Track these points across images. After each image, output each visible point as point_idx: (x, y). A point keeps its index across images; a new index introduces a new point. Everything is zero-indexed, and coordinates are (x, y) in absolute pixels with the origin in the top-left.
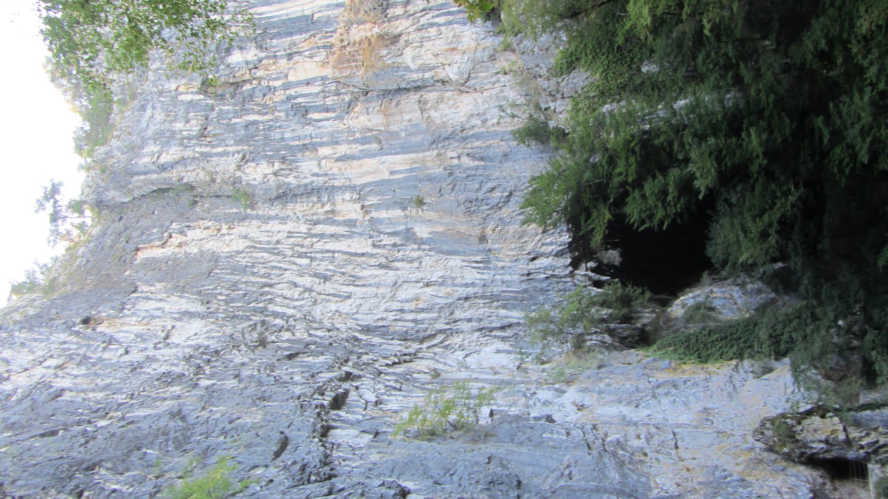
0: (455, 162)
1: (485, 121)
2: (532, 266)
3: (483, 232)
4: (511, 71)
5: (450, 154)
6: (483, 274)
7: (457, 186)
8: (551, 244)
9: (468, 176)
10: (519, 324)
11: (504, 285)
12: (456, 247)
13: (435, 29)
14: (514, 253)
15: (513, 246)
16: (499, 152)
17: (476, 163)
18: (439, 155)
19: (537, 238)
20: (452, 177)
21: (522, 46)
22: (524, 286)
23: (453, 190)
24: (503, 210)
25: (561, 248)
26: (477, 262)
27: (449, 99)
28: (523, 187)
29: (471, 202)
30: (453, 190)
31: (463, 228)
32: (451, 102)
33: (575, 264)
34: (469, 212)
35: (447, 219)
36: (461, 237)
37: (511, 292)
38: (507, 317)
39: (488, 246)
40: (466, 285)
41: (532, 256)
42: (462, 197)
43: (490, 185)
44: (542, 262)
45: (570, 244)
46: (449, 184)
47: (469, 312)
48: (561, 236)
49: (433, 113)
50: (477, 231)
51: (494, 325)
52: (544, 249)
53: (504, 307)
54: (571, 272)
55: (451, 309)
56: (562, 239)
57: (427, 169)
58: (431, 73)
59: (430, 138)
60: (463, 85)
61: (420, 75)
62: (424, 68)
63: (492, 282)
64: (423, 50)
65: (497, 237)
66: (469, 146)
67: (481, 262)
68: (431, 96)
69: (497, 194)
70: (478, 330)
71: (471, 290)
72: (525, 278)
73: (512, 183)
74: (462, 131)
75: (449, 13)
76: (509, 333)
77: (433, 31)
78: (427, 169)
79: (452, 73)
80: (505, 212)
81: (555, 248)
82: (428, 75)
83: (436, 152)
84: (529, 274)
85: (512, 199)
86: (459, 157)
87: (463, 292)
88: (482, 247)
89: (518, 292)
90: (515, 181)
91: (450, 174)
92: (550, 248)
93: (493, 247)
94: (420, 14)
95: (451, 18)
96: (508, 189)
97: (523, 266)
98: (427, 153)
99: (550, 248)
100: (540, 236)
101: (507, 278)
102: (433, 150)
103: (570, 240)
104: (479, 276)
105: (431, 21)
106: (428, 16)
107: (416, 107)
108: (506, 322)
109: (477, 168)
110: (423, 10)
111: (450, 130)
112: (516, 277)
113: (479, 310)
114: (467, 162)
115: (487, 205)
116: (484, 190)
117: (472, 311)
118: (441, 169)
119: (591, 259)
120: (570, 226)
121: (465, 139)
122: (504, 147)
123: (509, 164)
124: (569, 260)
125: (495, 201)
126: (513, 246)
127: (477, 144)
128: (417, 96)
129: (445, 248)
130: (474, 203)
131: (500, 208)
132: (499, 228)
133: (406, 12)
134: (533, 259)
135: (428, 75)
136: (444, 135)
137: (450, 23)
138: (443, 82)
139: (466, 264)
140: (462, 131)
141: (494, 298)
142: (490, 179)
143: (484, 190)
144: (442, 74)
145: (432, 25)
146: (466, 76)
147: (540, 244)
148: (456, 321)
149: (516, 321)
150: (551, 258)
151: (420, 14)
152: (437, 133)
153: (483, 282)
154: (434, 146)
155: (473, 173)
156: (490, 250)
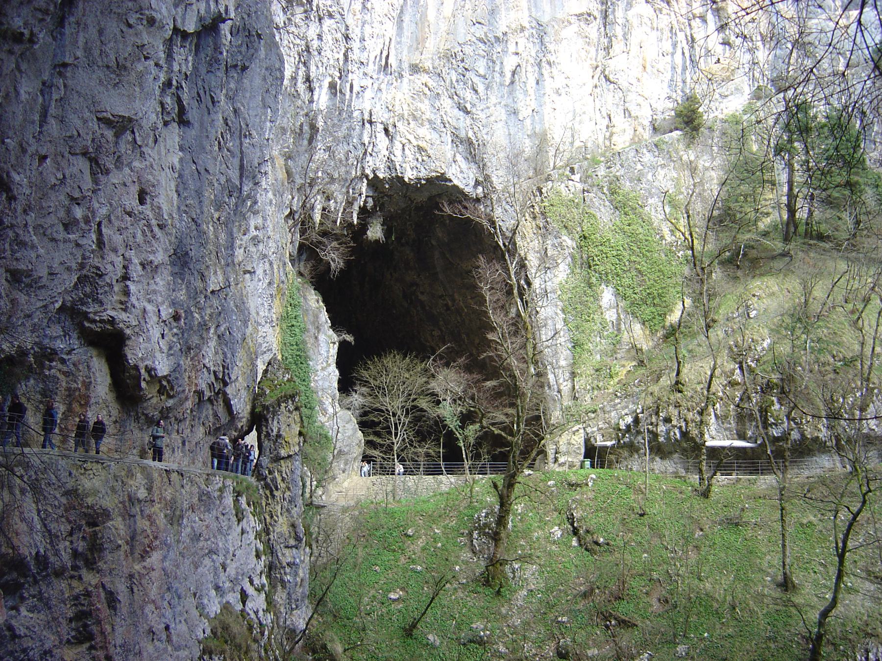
0: (512, 48)
1: (558, 92)
2: (380, 127)
3: (425, 71)
4: (612, 135)
5: (522, 42)
6: (374, 63)
7: (483, 47)
8: (404, 155)
9: (494, 62)
10: (311, 101)
11: (359, 89)
12: (407, 33)
13: (671, 50)
14: (397, 108)
15: (405, 107)
16: (520, 105)
17: (508, 75)
18: (523, 29)
19: (411, 138)
20: (493, 40)
21: (645, 151)
22: (356, 114)
23: (481, 40)
24: (450, 101)
25: (398, 167)
26: (387, 57)
27: (587, 52)
28: (476, 129)
29: (463, 61)
30: (481, 40)
31: (432, 45)
32: (583, 53)
33: (375, 183)
34: (449, 56)
35: (443, 27)
36: (419, 43)
37: (351, 97)
38: (320, 87)
39: (406, 74)
40: (363, 40)
41: (390, 129)
42: (468, 50)
43: (481, 88)
44: (382, 141)
45: (400, 179)
46: (486, 35)
47: (329, 38)
48: (412, 169)
49: (574, 28)
50: (428, 65)
51: (313, 68)
52: (398, 146)
53: (332, 86)
54: (367, 177)
55: (338, 16)
56: (408, 169)
57: (507, 9)
58: (620, 37)
59: (545, 19)
60: (603, 72)
61: (620, 21)
62: (627, 25)
63: (365, 74)
64: (649, 30)
65: (417, 88)
66: (529, 69)
67: (387, 63)
68: (594, 30)
69: (469, 95)
70: (308, 46)
71: (355, 45)
72: (366, 117)
73: (482, 116)
74: (549, 63)
75: (684, 69)
76: (301, 87)
77: (667, 46)
78: (507, 9)
79: (617, 64)
80: (447, 103)
81: (398, 159)
82: (619, 31)
83: (527, 25)
84: (371, 122)
85: (461, 113)
86: (517, 54)
87: (355, 33)
88: (405, 66)
89: (349, 106)
90: (484, 121)
91: (497, 39)
92: (398, 152)
93: (405, 80)
94: (688, 34)
95: (679, 70)
96: (474, 110)
97: (381, 115)
98: (527, 13)
99: (398, 152)
100: (415, 143)
101: (369, 94)
102: (530, 22)
103: (406, 180)
104: (372, 59)
105: (679, 45)
106: (685, 42)
107: (584, 10)
108: (316, 85)
109: (502, 73)
110: (693, 40)
111: (551, 47)
112: (367, 106)
113: (332, 54)
114: (510, 63)
115: (457, 81)
116: (476, 80)
117: (331, 42)
118: (505, 29)
119: (375, 206)
120: (423, 182)
121: (539, 65)
122: (524, 112)
123: (504, 117)
124: (381, 176)
125: (461, 93)
126: (405, 107)
127: (532, 82)
128: (597, 14)
129: (407, 18)
130: (461, 65)
131: (451, 98)
132: (428, 92)
133: (694, 17)
134: (386, 130)
135: (619, 31)
136: (546, 39)
137: (674, 68)
138: (608, 49)
139: (387, 43)
140: (549, 63)
141: (343, 73)
142: (487, 89)
143: (476, 80)
144: (618, 46)
145: (675, 45)
146: (611, 77)
147: (404, 141)
148: (320, 19)
149: (315, 98)
150: (387, 153)
151: (688, 34)
152: (549, 30)
153: (365, 61)
154: (534, 24)
155: (497, 68)
156: (401, 76)
